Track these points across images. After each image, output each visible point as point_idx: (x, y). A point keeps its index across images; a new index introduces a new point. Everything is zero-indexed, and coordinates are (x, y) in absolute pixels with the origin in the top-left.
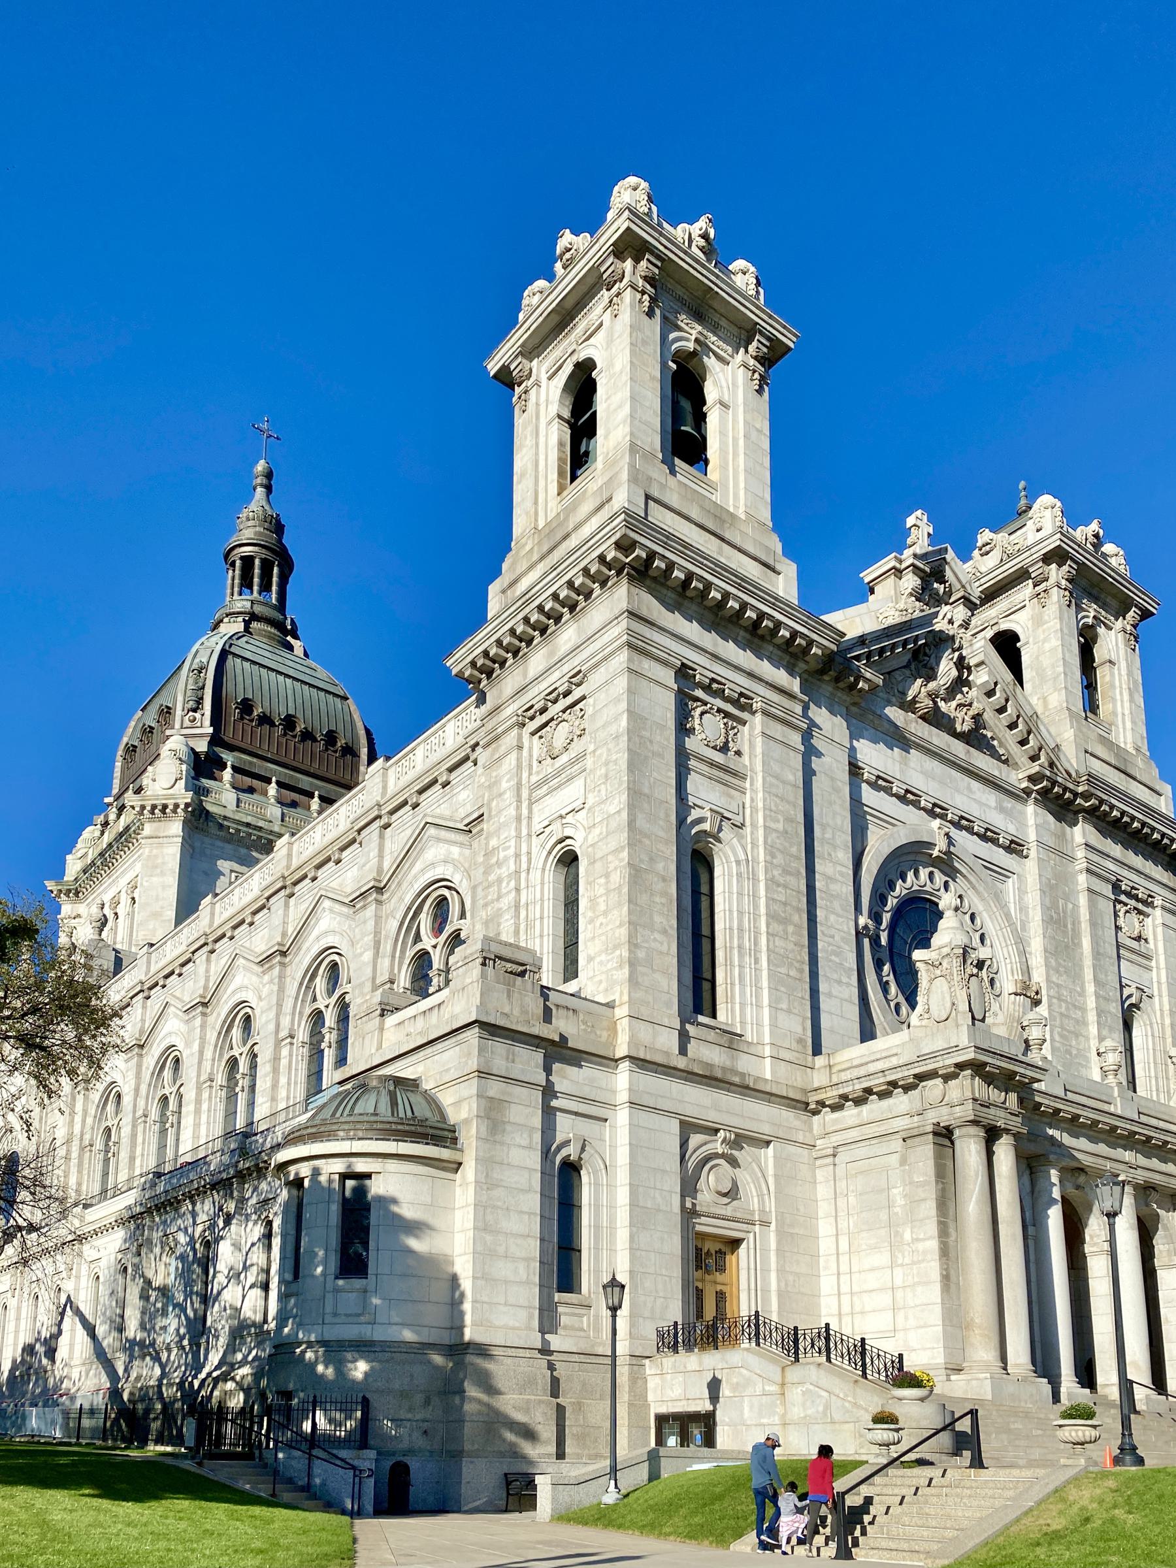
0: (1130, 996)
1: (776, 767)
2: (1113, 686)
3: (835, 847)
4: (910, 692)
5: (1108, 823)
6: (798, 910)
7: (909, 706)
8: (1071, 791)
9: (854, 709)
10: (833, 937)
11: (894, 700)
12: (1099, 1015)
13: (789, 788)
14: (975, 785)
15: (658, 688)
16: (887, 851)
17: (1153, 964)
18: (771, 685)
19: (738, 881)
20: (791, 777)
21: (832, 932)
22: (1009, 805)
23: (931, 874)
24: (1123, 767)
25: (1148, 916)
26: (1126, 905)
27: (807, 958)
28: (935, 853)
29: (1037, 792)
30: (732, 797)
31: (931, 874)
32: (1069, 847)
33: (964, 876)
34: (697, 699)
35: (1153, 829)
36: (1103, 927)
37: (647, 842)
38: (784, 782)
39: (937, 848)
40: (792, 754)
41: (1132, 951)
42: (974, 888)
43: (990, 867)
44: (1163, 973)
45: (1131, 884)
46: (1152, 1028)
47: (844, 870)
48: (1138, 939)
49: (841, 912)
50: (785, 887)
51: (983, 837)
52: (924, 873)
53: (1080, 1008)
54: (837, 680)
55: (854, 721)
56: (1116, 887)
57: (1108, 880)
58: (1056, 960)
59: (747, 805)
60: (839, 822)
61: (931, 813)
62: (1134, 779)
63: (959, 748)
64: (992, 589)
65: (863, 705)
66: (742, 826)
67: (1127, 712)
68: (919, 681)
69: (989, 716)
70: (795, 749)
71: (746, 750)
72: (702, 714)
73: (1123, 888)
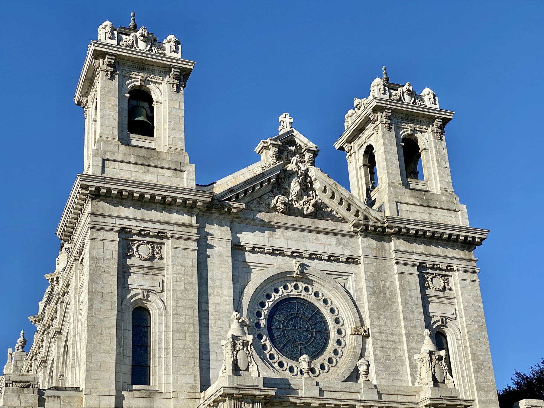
0: (438, 321)
1: (180, 261)
2: (428, 161)
3: (221, 288)
4: (272, 204)
5: (411, 236)
6: (193, 325)
7: (270, 210)
8: (380, 227)
9: (237, 220)
10: (219, 332)
11: (263, 209)
12: (407, 337)
13: (189, 268)
14: (321, 236)
15: (108, 243)
16: (260, 282)
17: (456, 301)
18: (176, 224)
19: (159, 318)
20: (190, 263)
21: (219, 329)
22: (346, 241)
23: (296, 287)
24: (425, 204)
25: (451, 276)
26: (433, 274)
27: (198, 347)
28: (295, 275)
29: (360, 231)
30: (155, 280)
31: (296, 287)
32: (387, 253)
33: (317, 282)
34: (135, 240)
35: (442, 234)
36: (410, 290)
37: (100, 313)
38: (185, 267)
39: (295, 273)
40: (190, 252)
41: (439, 297)
42: (323, 286)
43: (334, 274)
44: (462, 304)
45: (432, 263)
46: (456, 335)
47: (227, 298)
48: (444, 289)
49: (224, 318)
50: (185, 315)
51: (329, 260)
52: (290, 286)
53: (396, 335)
54: (220, 210)
55: (238, 225)
56: (422, 267)
57: (413, 265)
58: (378, 313)
59: (165, 282)
60: (224, 275)
61: (292, 255)
62: (436, 208)
63: (307, 222)
64: (360, 127)
65: (241, 216)
66: (162, 291)
67: (437, 172)
68: (277, 197)
69: (327, 201)
70: (192, 250)
71: (164, 256)
72: (138, 246)
73: (427, 266)
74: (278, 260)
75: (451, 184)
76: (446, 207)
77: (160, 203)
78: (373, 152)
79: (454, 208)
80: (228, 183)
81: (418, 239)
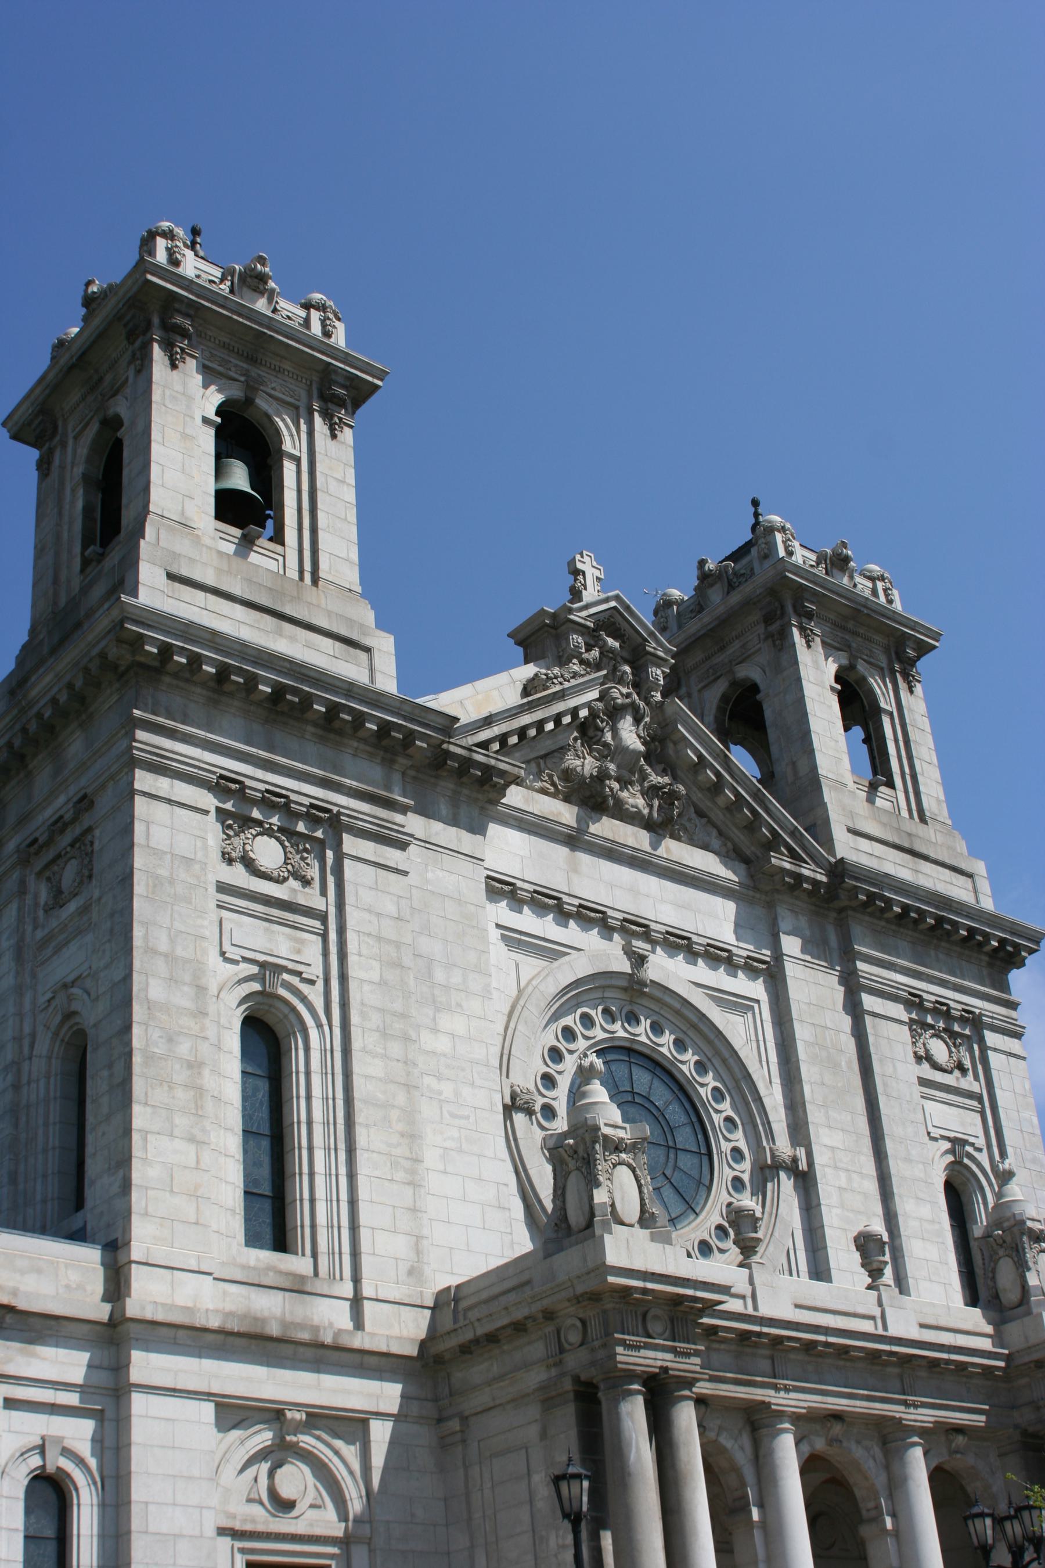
10: (467, 1118)
20: (391, 908)
35: (955, 925)
38: (378, 915)
50: (385, 1056)
57: (895, 998)
74: (591, 940)
75: (944, 805)
76: (948, 861)
77: (315, 725)
78: (758, 697)
79: (963, 866)
80: (466, 702)
81: (902, 930)
